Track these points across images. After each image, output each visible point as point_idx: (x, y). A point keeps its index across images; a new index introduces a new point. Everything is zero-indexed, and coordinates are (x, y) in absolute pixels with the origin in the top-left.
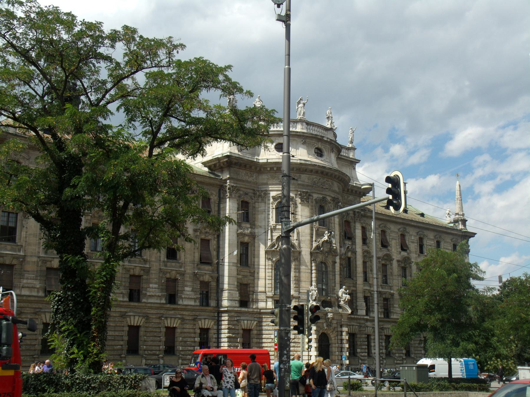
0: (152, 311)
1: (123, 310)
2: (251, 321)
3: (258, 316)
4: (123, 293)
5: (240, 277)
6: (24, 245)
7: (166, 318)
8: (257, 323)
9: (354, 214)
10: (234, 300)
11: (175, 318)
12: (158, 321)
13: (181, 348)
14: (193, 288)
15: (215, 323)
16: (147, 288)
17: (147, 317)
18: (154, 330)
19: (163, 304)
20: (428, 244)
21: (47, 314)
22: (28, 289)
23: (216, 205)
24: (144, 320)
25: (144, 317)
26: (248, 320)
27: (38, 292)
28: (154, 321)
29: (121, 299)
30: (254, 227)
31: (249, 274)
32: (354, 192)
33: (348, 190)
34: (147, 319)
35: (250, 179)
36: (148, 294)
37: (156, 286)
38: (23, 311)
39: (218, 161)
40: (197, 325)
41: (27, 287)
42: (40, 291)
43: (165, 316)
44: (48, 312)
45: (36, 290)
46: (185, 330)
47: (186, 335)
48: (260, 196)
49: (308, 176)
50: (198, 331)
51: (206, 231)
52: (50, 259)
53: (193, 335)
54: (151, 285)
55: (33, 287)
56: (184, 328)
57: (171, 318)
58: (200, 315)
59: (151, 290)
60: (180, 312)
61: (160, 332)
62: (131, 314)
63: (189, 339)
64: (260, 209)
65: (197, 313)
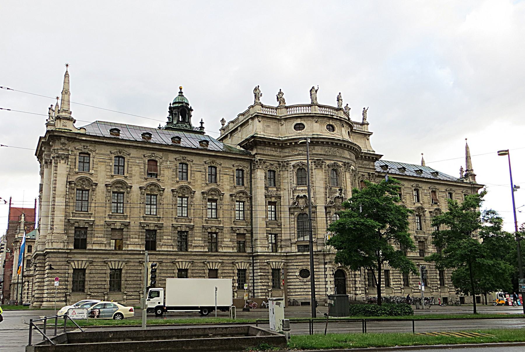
1: (173, 257)
3: (285, 258)
4: (172, 245)
6: (94, 213)
8: (284, 264)
9: (369, 175)
10: (264, 247)
11: (216, 262)
12: (202, 265)
18: (200, 271)
19: (206, 252)
20: (440, 195)
21: (112, 262)
23: (248, 175)
24: (190, 264)
27: (105, 246)
28: (199, 265)
29: (172, 250)
30: (279, 190)
31: (277, 226)
33: (362, 156)
36: (193, 245)
37: (200, 239)
38: (94, 261)
41: (97, 243)
43: (207, 261)
44: (113, 261)
46: (225, 271)
48: (283, 166)
50: (237, 272)
51: (240, 195)
52: (113, 223)
53: (232, 275)
54: (196, 238)
55: (101, 243)
56: (224, 270)
60: (220, 257)
65: (235, 258)
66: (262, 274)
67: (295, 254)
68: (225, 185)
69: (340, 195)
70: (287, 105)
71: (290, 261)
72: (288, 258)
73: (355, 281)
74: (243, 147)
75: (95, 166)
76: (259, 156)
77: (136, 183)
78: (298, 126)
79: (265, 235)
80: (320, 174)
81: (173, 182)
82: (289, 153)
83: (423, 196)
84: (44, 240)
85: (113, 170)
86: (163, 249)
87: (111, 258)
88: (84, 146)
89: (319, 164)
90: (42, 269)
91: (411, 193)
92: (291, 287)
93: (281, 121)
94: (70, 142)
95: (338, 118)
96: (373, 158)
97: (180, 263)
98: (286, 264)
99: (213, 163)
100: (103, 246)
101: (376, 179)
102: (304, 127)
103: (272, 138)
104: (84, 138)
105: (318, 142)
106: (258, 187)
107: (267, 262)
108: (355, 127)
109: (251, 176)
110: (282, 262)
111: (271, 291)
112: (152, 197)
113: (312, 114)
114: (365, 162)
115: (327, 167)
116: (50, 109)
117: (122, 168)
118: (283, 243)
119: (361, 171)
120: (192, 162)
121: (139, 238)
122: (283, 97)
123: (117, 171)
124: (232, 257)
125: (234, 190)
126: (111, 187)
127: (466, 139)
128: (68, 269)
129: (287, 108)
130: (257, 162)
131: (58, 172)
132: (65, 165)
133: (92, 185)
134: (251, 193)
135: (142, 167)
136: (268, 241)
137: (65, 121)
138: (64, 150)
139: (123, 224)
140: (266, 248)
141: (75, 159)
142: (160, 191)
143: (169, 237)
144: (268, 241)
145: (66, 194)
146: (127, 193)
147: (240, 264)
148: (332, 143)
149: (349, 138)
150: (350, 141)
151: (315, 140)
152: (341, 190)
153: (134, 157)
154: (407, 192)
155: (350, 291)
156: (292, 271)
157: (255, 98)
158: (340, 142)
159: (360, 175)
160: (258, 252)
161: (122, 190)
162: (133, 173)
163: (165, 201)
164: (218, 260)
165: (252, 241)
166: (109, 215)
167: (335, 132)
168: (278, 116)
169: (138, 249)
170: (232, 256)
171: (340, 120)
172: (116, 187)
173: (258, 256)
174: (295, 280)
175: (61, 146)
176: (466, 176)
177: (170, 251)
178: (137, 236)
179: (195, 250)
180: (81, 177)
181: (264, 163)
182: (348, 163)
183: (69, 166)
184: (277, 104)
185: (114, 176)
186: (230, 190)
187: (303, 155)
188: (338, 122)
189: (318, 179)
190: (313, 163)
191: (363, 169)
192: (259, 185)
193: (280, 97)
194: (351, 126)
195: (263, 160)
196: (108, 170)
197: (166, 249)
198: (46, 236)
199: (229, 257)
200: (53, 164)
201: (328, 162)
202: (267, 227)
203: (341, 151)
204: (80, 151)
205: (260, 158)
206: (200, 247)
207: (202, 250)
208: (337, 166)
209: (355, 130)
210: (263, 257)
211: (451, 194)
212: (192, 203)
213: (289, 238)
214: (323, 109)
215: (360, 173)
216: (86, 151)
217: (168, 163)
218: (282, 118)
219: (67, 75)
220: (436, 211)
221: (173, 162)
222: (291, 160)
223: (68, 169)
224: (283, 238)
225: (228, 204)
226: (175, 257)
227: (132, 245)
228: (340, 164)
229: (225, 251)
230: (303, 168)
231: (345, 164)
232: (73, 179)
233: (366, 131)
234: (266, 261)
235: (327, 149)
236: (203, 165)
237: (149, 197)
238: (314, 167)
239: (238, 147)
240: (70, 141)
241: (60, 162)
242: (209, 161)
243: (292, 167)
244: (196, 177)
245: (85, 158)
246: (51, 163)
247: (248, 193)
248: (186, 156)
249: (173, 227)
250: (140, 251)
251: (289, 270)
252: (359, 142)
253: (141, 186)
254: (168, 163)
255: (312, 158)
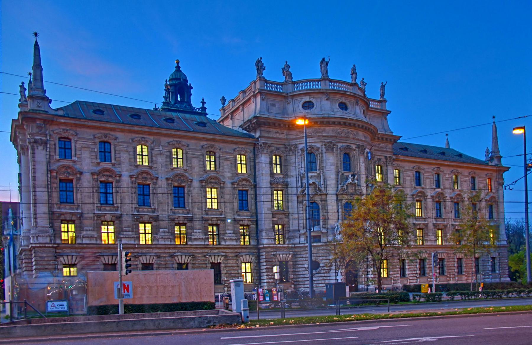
0: (198, 251)
1: (171, 251)
2: (287, 254)
5: (275, 219)
7: (210, 256)
10: (270, 239)
12: (204, 258)
13: (226, 279)
14: (234, 231)
15: (255, 257)
16: (191, 233)
17: (193, 256)
21: (105, 257)
22: (87, 238)
24: (190, 258)
25: (190, 256)
26: (283, 254)
27: (96, 240)
28: (200, 259)
29: (169, 243)
31: (284, 217)
32: (384, 139)
34: (193, 257)
35: (281, 136)
36: (193, 237)
37: (200, 231)
39: (250, 123)
40: (239, 260)
41: (87, 237)
42: (98, 240)
45: (95, 239)
46: (229, 265)
47: (230, 268)
49: (331, 128)
51: (243, 183)
53: (236, 268)
54: (195, 231)
55: (91, 237)
56: (228, 263)
57: (214, 255)
58: (241, 252)
59: (195, 234)
61: (207, 267)
62: (177, 254)
63: (233, 272)
64: (291, 161)
65: (239, 251)
66: (269, 267)
67: (304, 245)
68: (226, 172)
69: (353, 181)
70: (294, 80)
71: (299, 253)
72: (296, 250)
73: (368, 272)
74: (245, 129)
75: (78, 152)
76: (263, 139)
77: (126, 172)
78: (306, 105)
79: (271, 226)
80: (331, 158)
81: (167, 170)
82: (297, 135)
83: (445, 181)
84: (27, 234)
85: (98, 157)
86: (160, 243)
87: (104, 253)
88: (63, 130)
89: (330, 147)
90: (30, 265)
91: (432, 177)
92: (300, 279)
93: (287, 99)
94: (48, 126)
95: (352, 94)
96: (391, 140)
97: (180, 257)
98: (294, 256)
99: (212, 148)
100: (93, 240)
101: (394, 163)
102: (313, 106)
103: (277, 118)
104: (63, 121)
105: (329, 122)
106: (262, 174)
107: (274, 255)
108: (372, 105)
109: (254, 162)
110: (290, 254)
111: (279, 284)
112: (145, 187)
113: (323, 90)
114: (382, 145)
115: (339, 151)
116: (20, 86)
117: (109, 154)
118: (291, 234)
119: (378, 154)
120: (188, 146)
121: (132, 231)
122: (290, 70)
123: (103, 157)
124: (236, 250)
125: (236, 178)
126: (98, 175)
127: (494, 117)
128: (58, 265)
129: (294, 83)
130: (261, 146)
131: (36, 159)
132: (44, 152)
133: (76, 174)
134: (255, 181)
135: (132, 153)
136: (275, 233)
137: (39, 101)
138: (41, 134)
139: (115, 216)
140: (273, 240)
141: (55, 145)
142: (153, 179)
143: (166, 230)
144: (275, 233)
145: (48, 184)
146: (116, 182)
147: (244, 257)
148: (345, 123)
149: (364, 117)
150: (366, 121)
151: (326, 120)
152: (353, 175)
153: (122, 142)
154: (427, 177)
155: (362, 282)
156: (301, 263)
157: (258, 72)
158: (354, 122)
159: (376, 159)
160: (263, 244)
161: (110, 179)
162: (122, 160)
163: (159, 191)
164: (220, 253)
165: (257, 233)
166: (97, 207)
167: (349, 111)
168: (283, 93)
169: (133, 242)
170: (236, 248)
171: (354, 96)
172: (104, 175)
173: (264, 248)
174: (304, 273)
175: (37, 130)
176: (491, 159)
177: (168, 245)
178: (130, 229)
179: (195, 243)
180: (63, 165)
181: (269, 146)
182: (363, 146)
183: (48, 153)
184: (282, 79)
185: (101, 164)
186: (232, 178)
187: (312, 138)
188: (353, 100)
189: (329, 164)
190: (323, 146)
191: (380, 152)
192: (264, 172)
193: (286, 71)
194: (367, 105)
195: (267, 143)
196: (92, 157)
197: (163, 243)
198: (30, 230)
199: (232, 250)
200: (30, 151)
201: (340, 145)
202: (273, 217)
203: (354, 131)
204: (59, 136)
205: (263, 141)
206: (200, 240)
207: (203, 243)
208: (350, 149)
209: (372, 108)
210: (269, 249)
211: (473, 178)
212: (189, 193)
213: (297, 228)
214: (335, 84)
215: (376, 157)
216: (66, 135)
217: (161, 148)
218: (289, 95)
219: (36, 45)
220: (458, 197)
221: (166, 146)
222: (298, 143)
223: (48, 156)
224: (291, 228)
225: (230, 193)
226: (174, 251)
227: (126, 239)
228: (354, 147)
229: (227, 243)
230: (312, 153)
231: (358, 147)
232: (54, 167)
233: (383, 109)
234: (272, 254)
235: (339, 129)
236: (201, 150)
237: (141, 186)
238: (324, 150)
239: (240, 130)
240: (46, 125)
241: (38, 148)
242: (207, 146)
243: (300, 151)
244: (193, 164)
245: (67, 143)
246: (28, 149)
247: (252, 182)
248: (180, 140)
249: (169, 218)
250: (135, 245)
251: (298, 262)
252: (376, 122)
253: (131, 174)
254: (161, 148)
255: (323, 141)
